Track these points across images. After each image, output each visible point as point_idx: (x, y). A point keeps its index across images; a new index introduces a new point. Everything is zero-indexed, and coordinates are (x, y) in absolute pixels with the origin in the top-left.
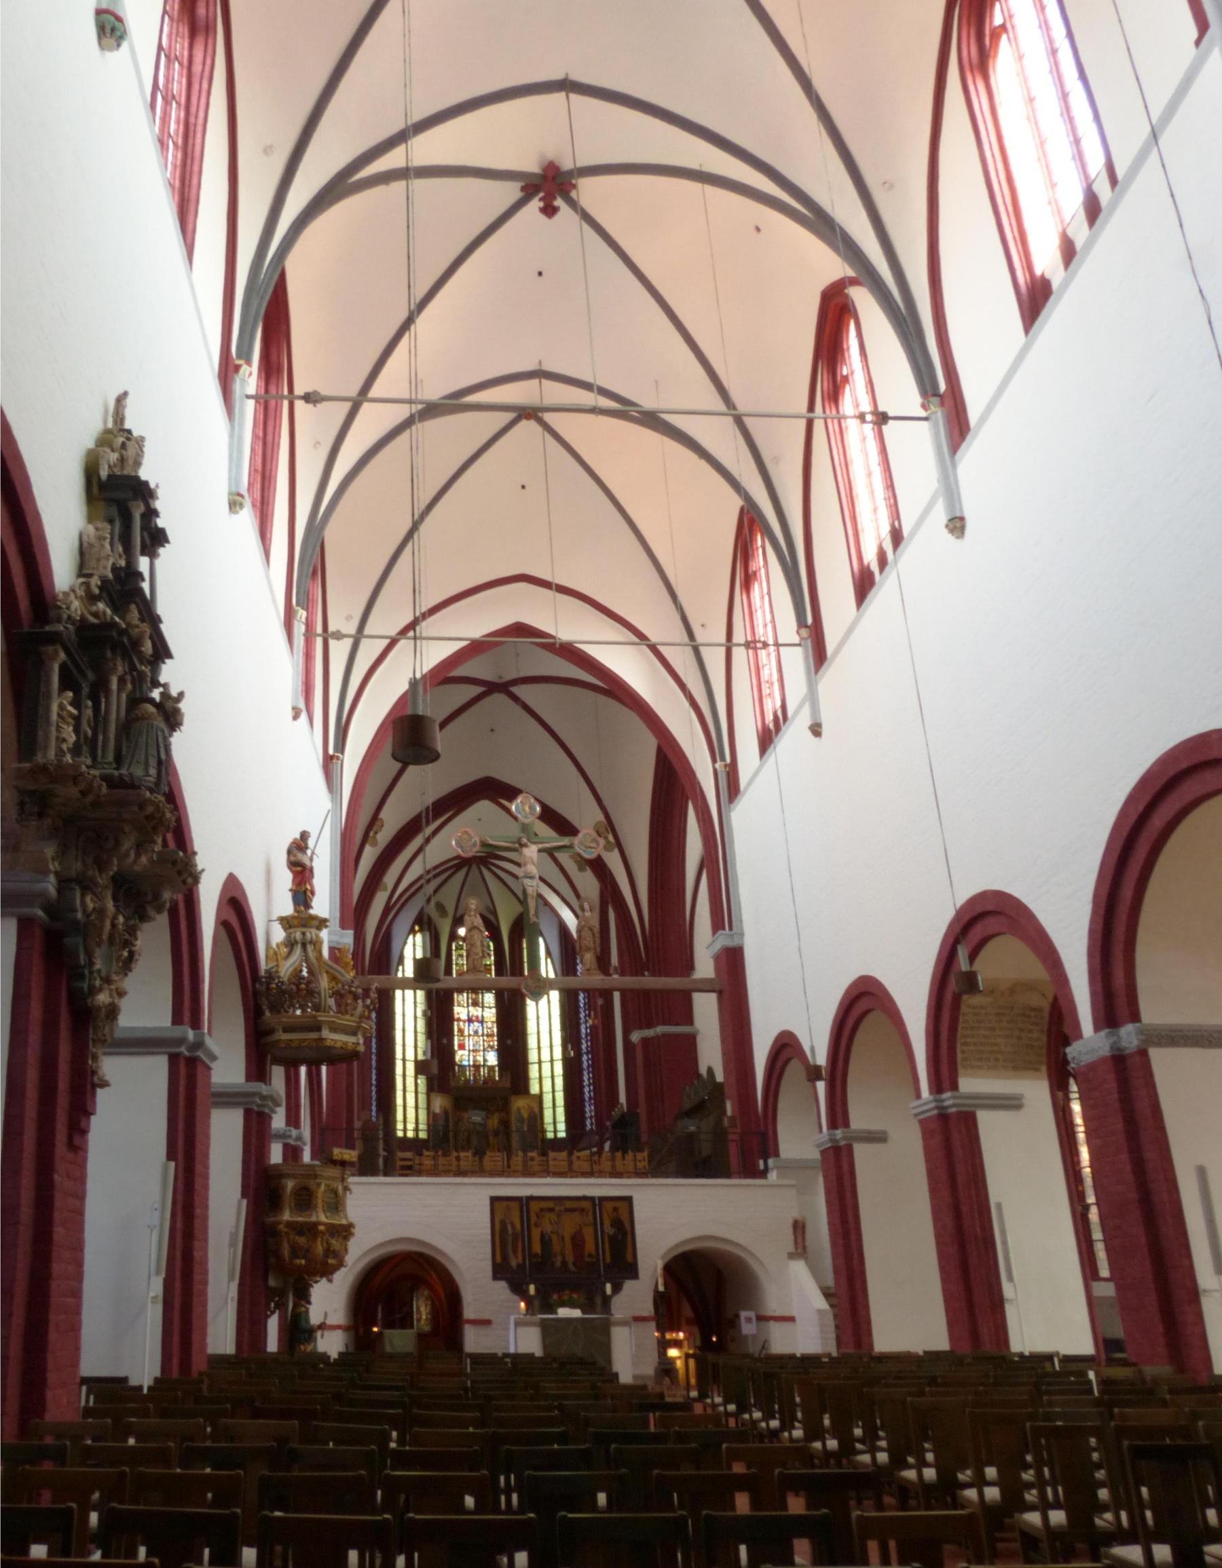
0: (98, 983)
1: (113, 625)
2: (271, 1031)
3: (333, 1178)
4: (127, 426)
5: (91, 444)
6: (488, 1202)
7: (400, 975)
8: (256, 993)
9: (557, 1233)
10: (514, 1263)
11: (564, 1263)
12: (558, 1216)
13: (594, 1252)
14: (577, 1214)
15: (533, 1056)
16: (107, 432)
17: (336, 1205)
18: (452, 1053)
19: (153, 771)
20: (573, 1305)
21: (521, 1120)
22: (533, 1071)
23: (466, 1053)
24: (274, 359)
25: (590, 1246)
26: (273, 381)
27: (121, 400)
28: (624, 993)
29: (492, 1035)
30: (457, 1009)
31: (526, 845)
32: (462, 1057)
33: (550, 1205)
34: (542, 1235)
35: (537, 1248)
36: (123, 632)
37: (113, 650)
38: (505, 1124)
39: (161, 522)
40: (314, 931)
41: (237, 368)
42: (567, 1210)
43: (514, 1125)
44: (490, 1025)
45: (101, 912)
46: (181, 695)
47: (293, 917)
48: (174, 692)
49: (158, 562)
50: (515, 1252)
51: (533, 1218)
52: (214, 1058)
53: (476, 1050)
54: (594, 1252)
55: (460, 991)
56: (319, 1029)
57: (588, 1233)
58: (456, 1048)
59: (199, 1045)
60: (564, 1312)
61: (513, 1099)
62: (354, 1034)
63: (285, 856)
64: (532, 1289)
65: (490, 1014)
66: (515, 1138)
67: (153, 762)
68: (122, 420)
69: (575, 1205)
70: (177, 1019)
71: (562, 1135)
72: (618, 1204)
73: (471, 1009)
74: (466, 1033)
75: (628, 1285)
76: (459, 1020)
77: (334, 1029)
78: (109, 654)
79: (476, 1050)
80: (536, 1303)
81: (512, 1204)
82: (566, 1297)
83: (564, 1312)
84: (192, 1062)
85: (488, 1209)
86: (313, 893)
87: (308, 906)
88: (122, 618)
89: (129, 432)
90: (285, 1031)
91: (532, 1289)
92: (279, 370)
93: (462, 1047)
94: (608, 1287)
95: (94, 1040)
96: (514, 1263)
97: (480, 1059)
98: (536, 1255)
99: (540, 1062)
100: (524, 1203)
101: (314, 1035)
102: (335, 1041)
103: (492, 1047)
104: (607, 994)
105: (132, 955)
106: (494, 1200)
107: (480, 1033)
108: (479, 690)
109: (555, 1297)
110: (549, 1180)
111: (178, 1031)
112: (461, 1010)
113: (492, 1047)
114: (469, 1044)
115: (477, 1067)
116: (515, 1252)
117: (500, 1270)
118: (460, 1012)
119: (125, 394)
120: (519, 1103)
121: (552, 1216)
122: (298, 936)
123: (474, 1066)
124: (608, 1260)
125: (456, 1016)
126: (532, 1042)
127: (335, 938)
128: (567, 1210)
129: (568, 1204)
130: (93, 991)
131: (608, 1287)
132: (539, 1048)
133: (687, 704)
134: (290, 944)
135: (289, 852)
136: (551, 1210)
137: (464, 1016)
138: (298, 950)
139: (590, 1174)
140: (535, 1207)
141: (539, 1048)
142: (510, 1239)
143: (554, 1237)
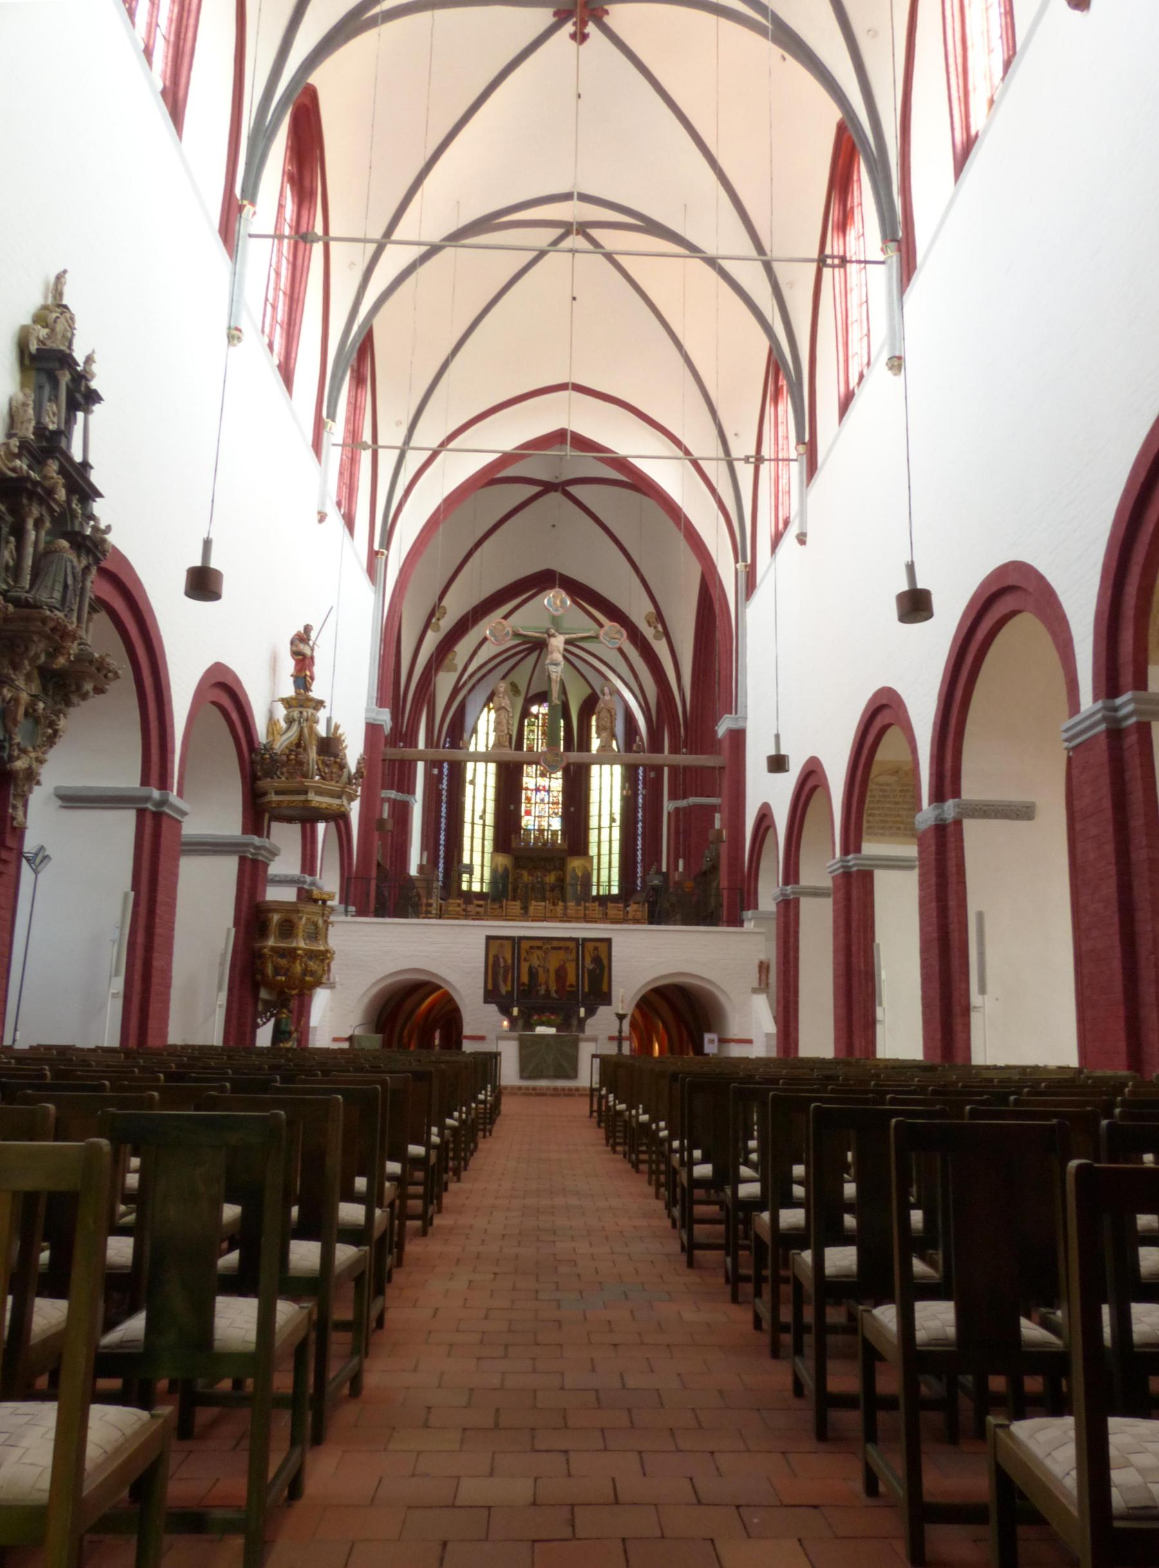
0: (16, 753)
1: (28, 478)
2: (265, 794)
3: (314, 913)
4: (64, 302)
5: (27, 320)
6: (483, 941)
7: (472, 749)
8: (252, 762)
9: (544, 967)
10: (504, 990)
11: (548, 991)
12: (546, 953)
13: (574, 983)
14: (562, 952)
15: (593, 822)
16: (45, 308)
17: (317, 933)
18: (519, 818)
19: (57, 595)
20: (550, 1025)
21: (575, 877)
22: (593, 836)
23: (532, 818)
24: (307, 182)
25: (571, 978)
26: (306, 205)
27: (60, 278)
28: (645, 766)
29: (557, 803)
30: (525, 780)
31: (553, 636)
32: (527, 822)
33: (539, 943)
34: (530, 968)
35: (525, 978)
36: (36, 484)
37: (30, 499)
38: (561, 880)
39: (94, 384)
40: (310, 711)
41: (241, 208)
42: (554, 948)
43: (568, 880)
44: (555, 794)
45: (16, 700)
46: (109, 528)
47: (291, 698)
48: (102, 526)
49: (91, 417)
50: (505, 981)
51: (524, 955)
52: (184, 814)
53: (542, 814)
54: (574, 983)
55: (530, 763)
56: (306, 793)
57: (571, 968)
58: (523, 813)
59: (164, 802)
60: (540, 1030)
61: (569, 859)
62: (340, 797)
63: (289, 646)
64: (515, 1011)
66: (569, 890)
67: (59, 587)
68: (61, 294)
69: (562, 944)
70: (145, 781)
71: (615, 891)
72: (597, 944)
73: (539, 779)
74: (533, 801)
75: (602, 1010)
76: (527, 789)
77: (320, 792)
78: (25, 501)
80: (520, 1023)
81: (505, 942)
82: (544, 1019)
83: (540, 1030)
84: (158, 816)
85: (483, 946)
86: (312, 678)
87: (307, 689)
88: (40, 472)
89: (65, 307)
90: (277, 793)
91: (515, 1011)
92: (313, 194)
93: (528, 813)
94: (582, 1011)
95: (14, 795)
96: (504, 990)
97: (545, 825)
98: (523, 984)
99: (600, 828)
100: (516, 942)
101: (302, 798)
102: (320, 803)
103: (556, 814)
104: (658, 769)
105: (56, 732)
106: (489, 939)
107: (546, 800)
108: (536, 489)
109: (535, 1017)
110: (545, 924)
111: (144, 792)
112: (530, 779)
113: (556, 814)
114: (536, 810)
115: (541, 831)
116: (505, 981)
117: (491, 995)
118: (528, 781)
119: (65, 272)
120: (575, 863)
121: (540, 953)
122: (296, 714)
123: (539, 830)
124: (586, 990)
125: (524, 786)
126: (594, 810)
127: (373, 715)
128: (554, 948)
129: (555, 944)
130: (11, 758)
131: (582, 1011)
132: (600, 816)
133: (715, 506)
134: (290, 721)
135: (292, 643)
136: (539, 948)
137: (532, 786)
138: (295, 727)
139: (544, 919)
140: (525, 945)
141: (600, 816)
142: (502, 970)
143: (540, 970)
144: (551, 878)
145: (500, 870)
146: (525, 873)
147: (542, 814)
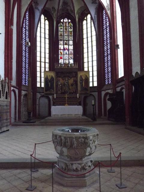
21: (82, 80)
23: (63, 60)
29: (72, 54)
30: (60, 46)
32: (61, 61)
38: (76, 82)
44: (71, 51)
53: (66, 58)
58: (59, 59)
65: (71, 48)
73: (65, 46)
76: (61, 49)
79: (66, 58)
93: (61, 58)
113: (72, 58)
137: (62, 48)
144: (71, 81)
145: (49, 78)
146: (61, 79)
147: (66, 50)
